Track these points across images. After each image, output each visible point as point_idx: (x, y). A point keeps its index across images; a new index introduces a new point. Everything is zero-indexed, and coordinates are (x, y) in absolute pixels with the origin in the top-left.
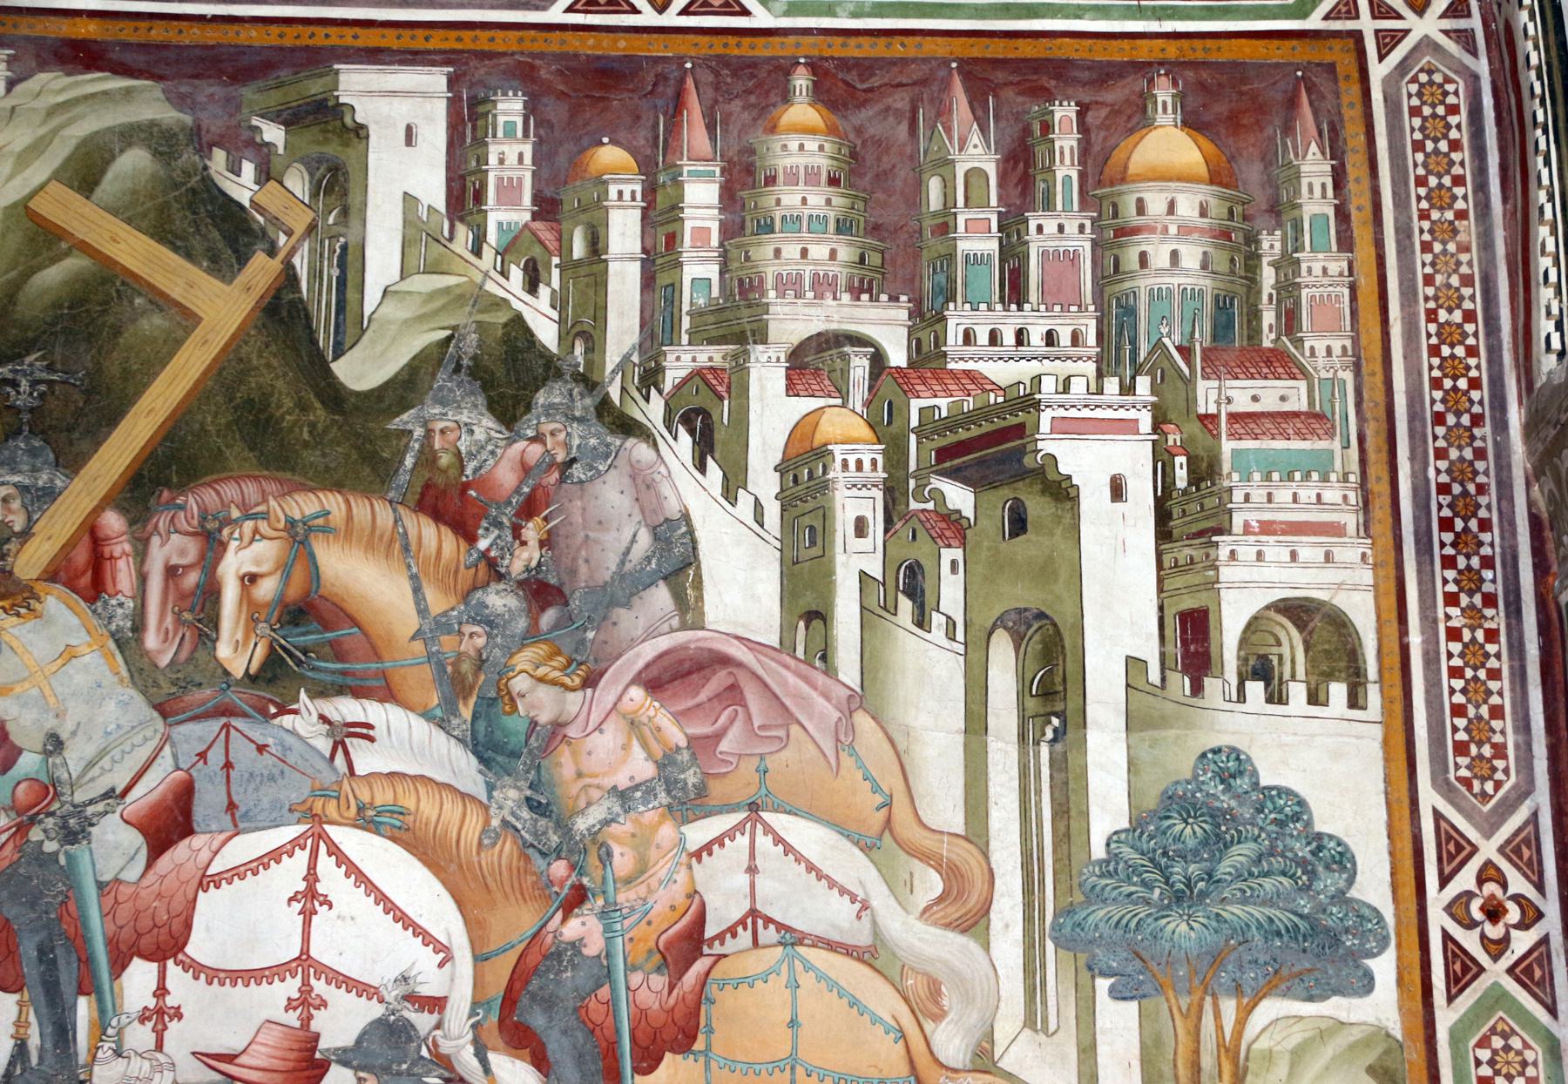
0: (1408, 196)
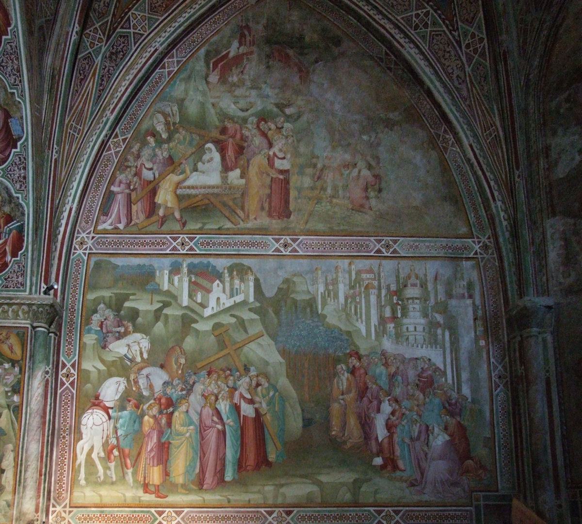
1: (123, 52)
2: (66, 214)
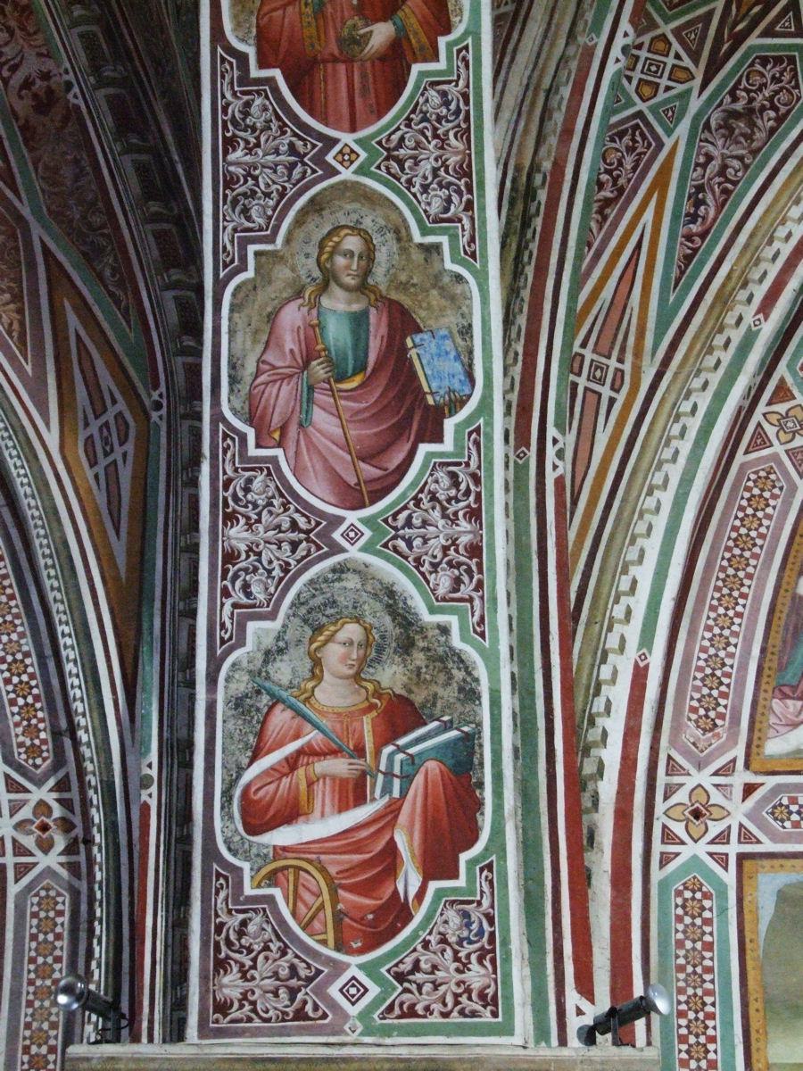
0: (22, 969)
1: (776, 109)
2: (619, 694)
